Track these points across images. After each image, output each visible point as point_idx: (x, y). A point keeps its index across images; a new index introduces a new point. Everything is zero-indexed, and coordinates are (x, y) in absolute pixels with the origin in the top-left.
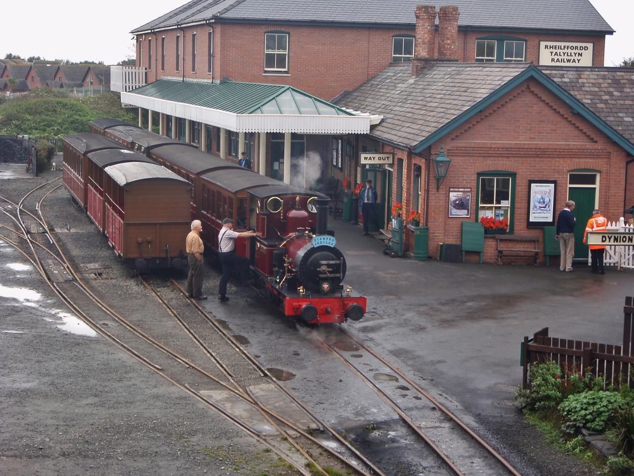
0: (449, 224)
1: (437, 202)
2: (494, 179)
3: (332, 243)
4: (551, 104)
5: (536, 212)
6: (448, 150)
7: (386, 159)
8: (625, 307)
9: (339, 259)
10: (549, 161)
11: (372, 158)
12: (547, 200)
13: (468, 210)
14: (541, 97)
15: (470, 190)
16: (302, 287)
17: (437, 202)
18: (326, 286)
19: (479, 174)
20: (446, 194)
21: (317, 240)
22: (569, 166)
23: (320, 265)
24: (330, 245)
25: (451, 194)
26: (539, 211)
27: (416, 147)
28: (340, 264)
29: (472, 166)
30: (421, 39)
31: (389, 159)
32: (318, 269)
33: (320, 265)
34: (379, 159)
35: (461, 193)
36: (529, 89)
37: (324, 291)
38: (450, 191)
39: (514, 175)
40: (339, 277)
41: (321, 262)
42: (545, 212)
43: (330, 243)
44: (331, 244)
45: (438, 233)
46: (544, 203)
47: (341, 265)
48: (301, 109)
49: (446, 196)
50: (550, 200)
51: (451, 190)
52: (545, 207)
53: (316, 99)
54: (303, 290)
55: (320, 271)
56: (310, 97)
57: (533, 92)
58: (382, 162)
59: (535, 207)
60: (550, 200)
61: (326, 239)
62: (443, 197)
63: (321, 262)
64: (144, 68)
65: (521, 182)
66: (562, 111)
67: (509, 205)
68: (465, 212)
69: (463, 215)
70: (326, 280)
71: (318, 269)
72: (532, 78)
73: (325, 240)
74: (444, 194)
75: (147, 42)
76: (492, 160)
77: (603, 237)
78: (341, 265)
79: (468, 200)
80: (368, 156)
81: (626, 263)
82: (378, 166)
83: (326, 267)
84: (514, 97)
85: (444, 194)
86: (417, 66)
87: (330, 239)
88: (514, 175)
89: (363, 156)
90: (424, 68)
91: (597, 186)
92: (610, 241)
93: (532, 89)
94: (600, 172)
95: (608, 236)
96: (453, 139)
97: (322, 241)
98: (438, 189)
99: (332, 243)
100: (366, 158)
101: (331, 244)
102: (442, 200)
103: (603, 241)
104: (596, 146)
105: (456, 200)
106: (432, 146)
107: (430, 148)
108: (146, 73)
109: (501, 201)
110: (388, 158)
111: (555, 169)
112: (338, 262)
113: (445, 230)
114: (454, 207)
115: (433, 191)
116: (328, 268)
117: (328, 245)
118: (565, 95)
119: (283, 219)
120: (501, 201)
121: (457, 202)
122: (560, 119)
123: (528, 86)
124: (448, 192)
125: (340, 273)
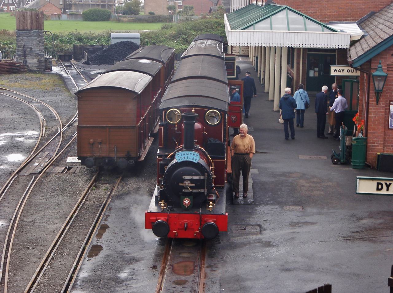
0: (389, 135)
1: (377, 114)
3: (196, 159)
6: (388, 65)
8: (389, 279)
9: (203, 175)
11: (341, 71)
16: (163, 201)
17: (377, 114)
18: (187, 201)
20: (386, 106)
21: (180, 155)
23: (183, 181)
24: (194, 161)
27: (354, 61)
28: (204, 180)
31: (344, 71)
32: (181, 184)
33: (183, 181)
34: (348, 71)
37: (185, 207)
40: (204, 193)
41: (184, 177)
43: (193, 158)
44: (195, 159)
45: (377, 143)
47: (206, 181)
48: (291, 26)
49: (386, 109)
53: (306, 17)
54: (164, 204)
55: (183, 186)
56: (302, 16)
61: (189, 154)
62: (382, 109)
63: (184, 177)
70: (188, 195)
71: (181, 184)
73: (189, 156)
74: (383, 107)
77: (378, 184)
78: (206, 181)
80: (338, 68)
82: (355, 77)
83: (189, 182)
85: (383, 107)
87: (194, 155)
89: (332, 68)
92: (388, 190)
95: (386, 184)
97: (192, 157)
98: (378, 102)
99: (196, 159)
100: (335, 71)
101: (195, 159)
103: (378, 189)
106: (372, 61)
107: (370, 62)
112: (202, 178)
113: (384, 140)
115: (373, 103)
116: (191, 183)
117: (192, 160)
119: (178, 130)
124: (388, 105)
125: (204, 189)
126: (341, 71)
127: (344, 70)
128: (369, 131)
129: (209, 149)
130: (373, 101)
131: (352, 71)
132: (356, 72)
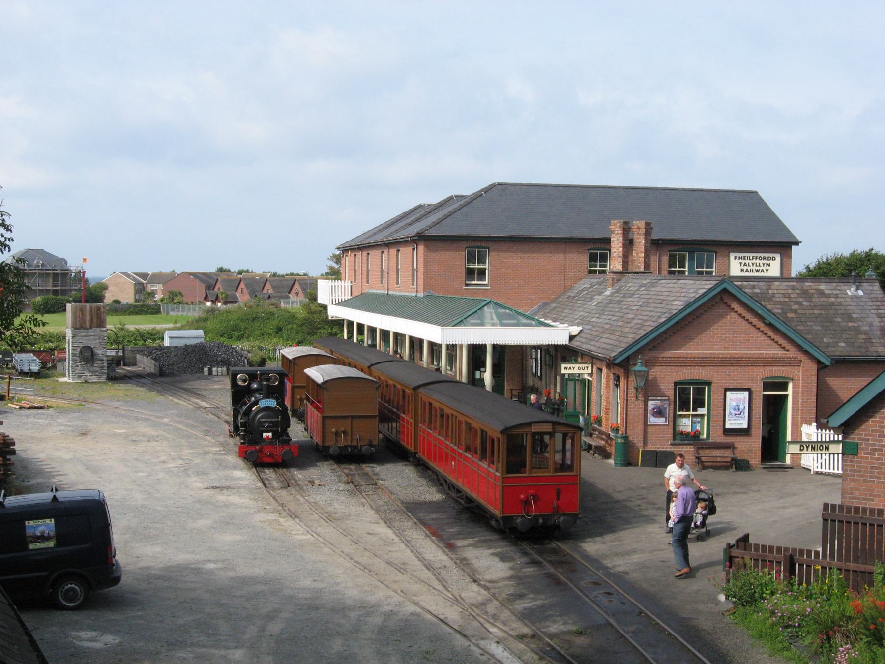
1: (636, 411)
4: (743, 315)
5: (731, 419)
6: (646, 360)
8: (823, 514)
10: (743, 370)
12: (742, 407)
13: (666, 418)
14: (734, 309)
19: (676, 384)
22: (762, 375)
26: (734, 418)
29: (669, 375)
34: (579, 369)
35: (659, 402)
36: (723, 300)
38: (648, 400)
39: (709, 384)
42: (740, 418)
46: (739, 410)
50: (745, 407)
51: (649, 398)
52: (739, 414)
57: (726, 303)
58: (581, 372)
59: (730, 414)
60: (745, 407)
64: (349, 282)
65: (717, 390)
66: (755, 321)
68: (663, 419)
72: (725, 291)
76: (688, 370)
77: (801, 446)
80: (568, 366)
84: (709, 308)
91: (790, 392)
92: (807, 450)
93: (725, 301)
96: (650, 350)
100: (566, 368)
102: (641, 408)
103: (801, 450)
105: (654, 409)
107: (628, 358)
108: (351, 286)
110: (587, 367)
111: (749, 377)
114: (653, 415)
118: (757, 306)
122: (753, 329)
123: (722, 298)
130: (632, 397)
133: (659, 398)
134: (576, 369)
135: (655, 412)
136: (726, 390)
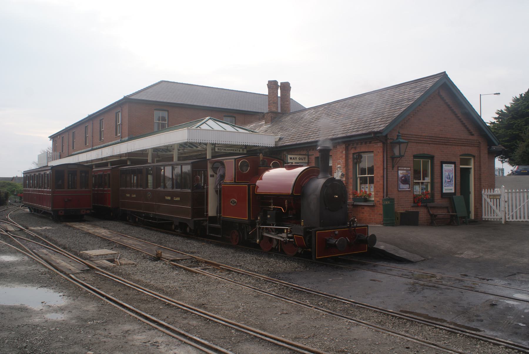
2: (421, 160)
5: (446, 185)
7: (304, 159)
11: (295, 158)
12: (451, 176)
13: (409, 185)
15: (409, 168)
25: (400, 172)
26: (447, 185)
30: (272, 100)
34: (300, 159)
35: (405, 171)
38: (398, 170)
39: (432, 158)
42: (450, 185)
46: (450, 179)
50: (453, 176)
51: (399, 168)
52: (450, 182)
59: (446, 182)
60: (453, 176)
64: (59, 153)
65: (437, 163)
67: (430, 181)
68: (407, 186)
69: (406, 189)
75: (61, 138)
79: (409, 176)
80: (292, 156)
81: (514, 217)
86: (271, 116)
88: (432, 158)
90: (275, 118)
91: (472, 166)
94: (474, 157)
100: (291, 158)
104: (471, 137)
105: (402, 177)
108: (60, 155)
109: (425, 178)
114: (401, 182)
120: (425, 178)
121: (403, 178)
126: (295, 158)
127: (297, 158)
128: (388, 193)
129: (237, 224)
131: (302, 159)
132: (305, 160)
133: (405, 168)
134: (297, 159)
135: (402, 180)
136: (442, 163)
